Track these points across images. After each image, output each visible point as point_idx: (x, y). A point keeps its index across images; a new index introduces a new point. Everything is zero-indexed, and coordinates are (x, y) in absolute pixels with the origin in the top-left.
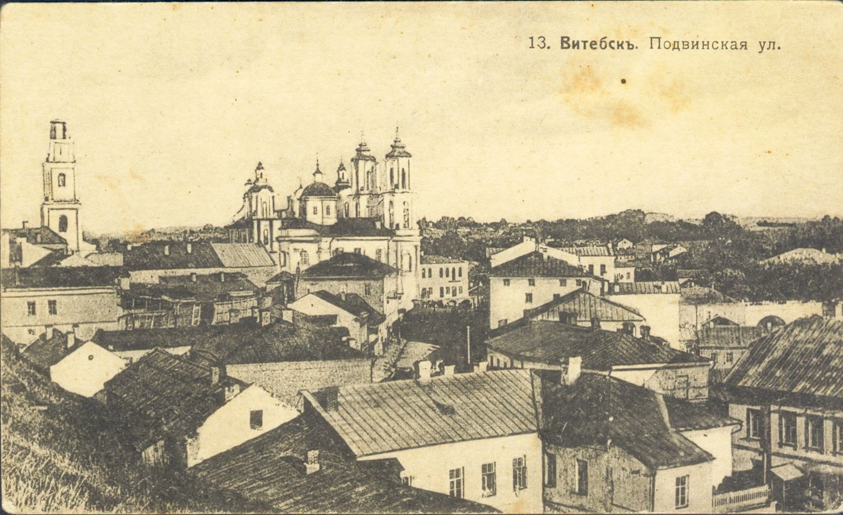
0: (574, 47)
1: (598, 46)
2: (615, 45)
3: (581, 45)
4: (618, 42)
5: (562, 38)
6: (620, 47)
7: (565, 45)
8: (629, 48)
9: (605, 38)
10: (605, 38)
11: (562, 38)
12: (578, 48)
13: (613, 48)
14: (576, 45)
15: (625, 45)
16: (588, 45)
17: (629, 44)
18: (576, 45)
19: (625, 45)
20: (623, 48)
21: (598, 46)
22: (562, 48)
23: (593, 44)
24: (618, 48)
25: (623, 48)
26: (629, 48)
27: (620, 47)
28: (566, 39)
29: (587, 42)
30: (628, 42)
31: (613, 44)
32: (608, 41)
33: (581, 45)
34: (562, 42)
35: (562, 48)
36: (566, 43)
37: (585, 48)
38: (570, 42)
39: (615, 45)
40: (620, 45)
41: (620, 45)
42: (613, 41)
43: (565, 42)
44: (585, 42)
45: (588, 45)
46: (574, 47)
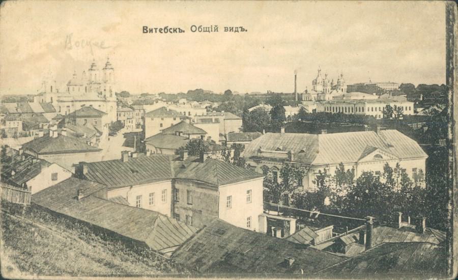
0: (150, 32)
1: (163, 31)
2: (172, 31)
3: (154, 30)
5: (144, 27)
7: (145, 31)
8: (180, 32)
9: (167, 27)
11: (144, 27)
13: (171, 32)
14: (151, 31)
15: (178, 30)
16: (158, 31)
18: (151, 31)
19: (178, 30)
20: (176, 32)
21: (163, 31)
22: (144, 32)
23: (160, 30)
25: (176, 32)
26: (180, 32)
28: (145, 28)
30: (179, 29)
32: (168, 28)
33: (154, 30)
34: (144, 29)
35: (144, 32)
36: (146, 29)
37: (156, 32)
38: (148, 29)
39: (172, 31)
40: (175, 30)
41: (175, 30)
44: (156, 29)
45: (158, 31)
46: (150, 32)
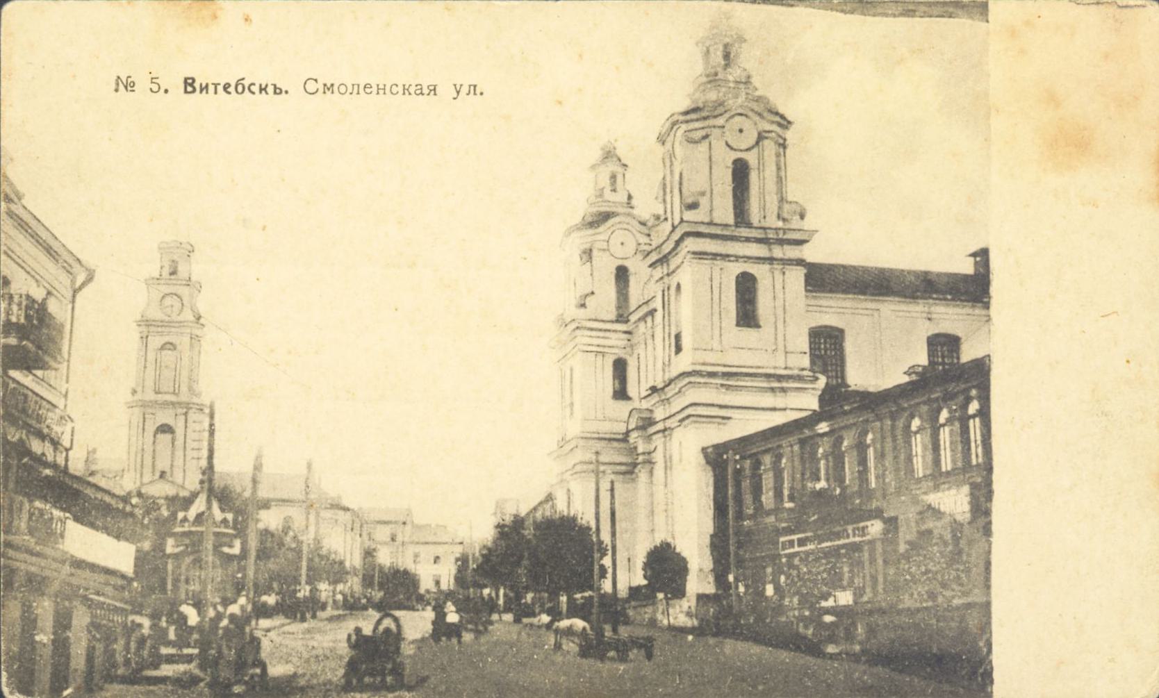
0: (201, 91)
2: (255, 89)
3: (211, 88)
4: (261, 85)
6: (263, 92)
7: (189, 89)
9: (243, 79)
10: (243, 79)
12: (207, 92)
14: (204, 88)
15: (270, 89)
16: (220, 88)
17: (275, 87)
18: (204, 88)
19: (270, 89)
22: (186, 92)
24: (261, 92)
27: (263, 92)
29: (219, 84)
30: (275, 86)
31: (253, 88)
32: (246, 83)
33: (211, 88)
35: (186, 92)
36: (191, 85)
38: (197, 85)
39: (254, 89)
40: (263, 89)
41: (263, 89)
42: (253, 84)
43: (189, 84)
45: (220, 88)
46: (201, 91)
